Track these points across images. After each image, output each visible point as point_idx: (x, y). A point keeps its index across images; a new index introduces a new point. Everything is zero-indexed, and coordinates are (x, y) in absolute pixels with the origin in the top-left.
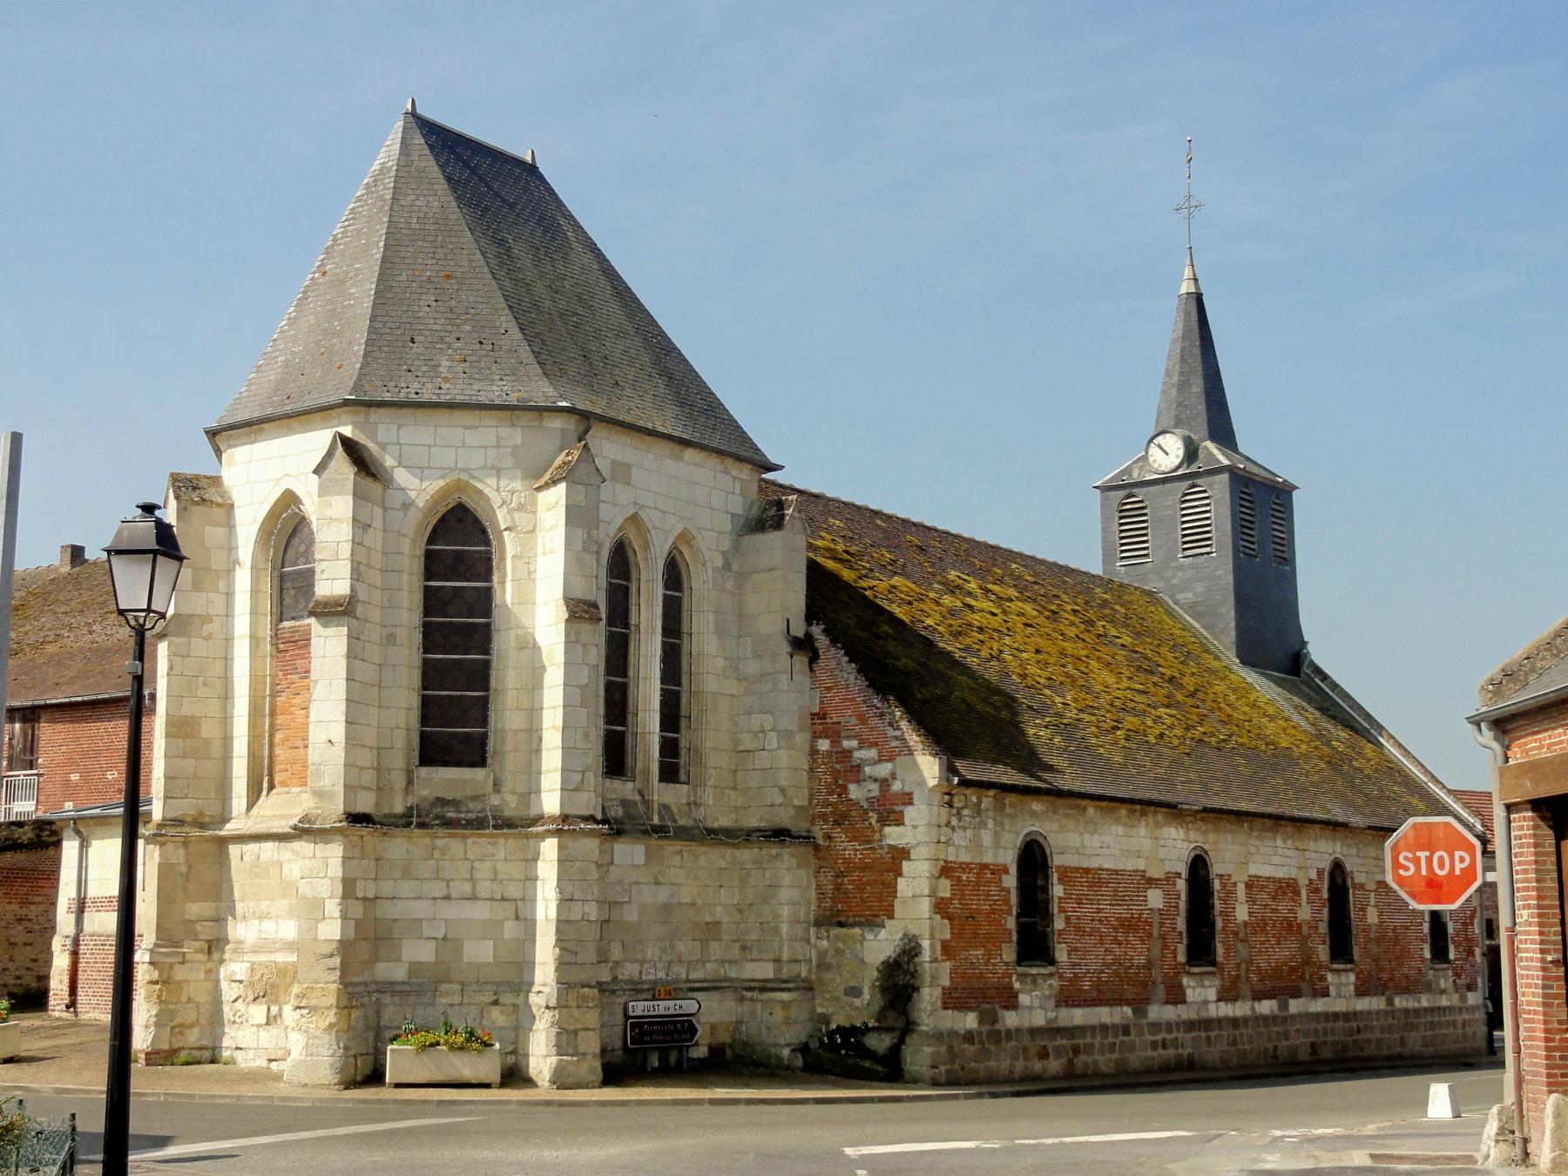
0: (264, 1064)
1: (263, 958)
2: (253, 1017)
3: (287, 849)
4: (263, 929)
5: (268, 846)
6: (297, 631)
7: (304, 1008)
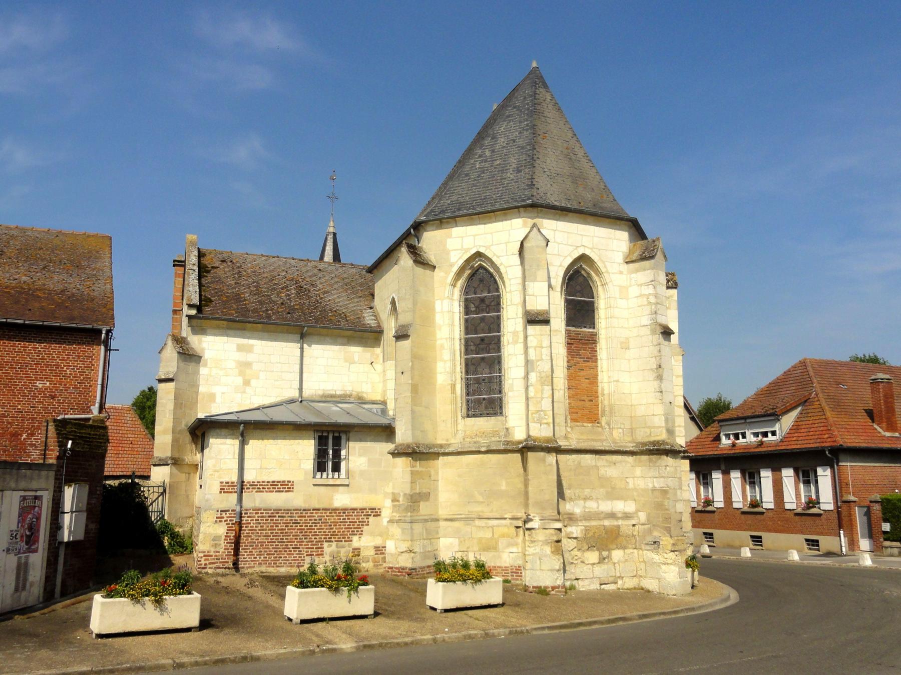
1: (594, 523)
3: (603, 460)
4: (587, 506)
5: (588, 457)
6: (580, 334)
7: (676, 551)
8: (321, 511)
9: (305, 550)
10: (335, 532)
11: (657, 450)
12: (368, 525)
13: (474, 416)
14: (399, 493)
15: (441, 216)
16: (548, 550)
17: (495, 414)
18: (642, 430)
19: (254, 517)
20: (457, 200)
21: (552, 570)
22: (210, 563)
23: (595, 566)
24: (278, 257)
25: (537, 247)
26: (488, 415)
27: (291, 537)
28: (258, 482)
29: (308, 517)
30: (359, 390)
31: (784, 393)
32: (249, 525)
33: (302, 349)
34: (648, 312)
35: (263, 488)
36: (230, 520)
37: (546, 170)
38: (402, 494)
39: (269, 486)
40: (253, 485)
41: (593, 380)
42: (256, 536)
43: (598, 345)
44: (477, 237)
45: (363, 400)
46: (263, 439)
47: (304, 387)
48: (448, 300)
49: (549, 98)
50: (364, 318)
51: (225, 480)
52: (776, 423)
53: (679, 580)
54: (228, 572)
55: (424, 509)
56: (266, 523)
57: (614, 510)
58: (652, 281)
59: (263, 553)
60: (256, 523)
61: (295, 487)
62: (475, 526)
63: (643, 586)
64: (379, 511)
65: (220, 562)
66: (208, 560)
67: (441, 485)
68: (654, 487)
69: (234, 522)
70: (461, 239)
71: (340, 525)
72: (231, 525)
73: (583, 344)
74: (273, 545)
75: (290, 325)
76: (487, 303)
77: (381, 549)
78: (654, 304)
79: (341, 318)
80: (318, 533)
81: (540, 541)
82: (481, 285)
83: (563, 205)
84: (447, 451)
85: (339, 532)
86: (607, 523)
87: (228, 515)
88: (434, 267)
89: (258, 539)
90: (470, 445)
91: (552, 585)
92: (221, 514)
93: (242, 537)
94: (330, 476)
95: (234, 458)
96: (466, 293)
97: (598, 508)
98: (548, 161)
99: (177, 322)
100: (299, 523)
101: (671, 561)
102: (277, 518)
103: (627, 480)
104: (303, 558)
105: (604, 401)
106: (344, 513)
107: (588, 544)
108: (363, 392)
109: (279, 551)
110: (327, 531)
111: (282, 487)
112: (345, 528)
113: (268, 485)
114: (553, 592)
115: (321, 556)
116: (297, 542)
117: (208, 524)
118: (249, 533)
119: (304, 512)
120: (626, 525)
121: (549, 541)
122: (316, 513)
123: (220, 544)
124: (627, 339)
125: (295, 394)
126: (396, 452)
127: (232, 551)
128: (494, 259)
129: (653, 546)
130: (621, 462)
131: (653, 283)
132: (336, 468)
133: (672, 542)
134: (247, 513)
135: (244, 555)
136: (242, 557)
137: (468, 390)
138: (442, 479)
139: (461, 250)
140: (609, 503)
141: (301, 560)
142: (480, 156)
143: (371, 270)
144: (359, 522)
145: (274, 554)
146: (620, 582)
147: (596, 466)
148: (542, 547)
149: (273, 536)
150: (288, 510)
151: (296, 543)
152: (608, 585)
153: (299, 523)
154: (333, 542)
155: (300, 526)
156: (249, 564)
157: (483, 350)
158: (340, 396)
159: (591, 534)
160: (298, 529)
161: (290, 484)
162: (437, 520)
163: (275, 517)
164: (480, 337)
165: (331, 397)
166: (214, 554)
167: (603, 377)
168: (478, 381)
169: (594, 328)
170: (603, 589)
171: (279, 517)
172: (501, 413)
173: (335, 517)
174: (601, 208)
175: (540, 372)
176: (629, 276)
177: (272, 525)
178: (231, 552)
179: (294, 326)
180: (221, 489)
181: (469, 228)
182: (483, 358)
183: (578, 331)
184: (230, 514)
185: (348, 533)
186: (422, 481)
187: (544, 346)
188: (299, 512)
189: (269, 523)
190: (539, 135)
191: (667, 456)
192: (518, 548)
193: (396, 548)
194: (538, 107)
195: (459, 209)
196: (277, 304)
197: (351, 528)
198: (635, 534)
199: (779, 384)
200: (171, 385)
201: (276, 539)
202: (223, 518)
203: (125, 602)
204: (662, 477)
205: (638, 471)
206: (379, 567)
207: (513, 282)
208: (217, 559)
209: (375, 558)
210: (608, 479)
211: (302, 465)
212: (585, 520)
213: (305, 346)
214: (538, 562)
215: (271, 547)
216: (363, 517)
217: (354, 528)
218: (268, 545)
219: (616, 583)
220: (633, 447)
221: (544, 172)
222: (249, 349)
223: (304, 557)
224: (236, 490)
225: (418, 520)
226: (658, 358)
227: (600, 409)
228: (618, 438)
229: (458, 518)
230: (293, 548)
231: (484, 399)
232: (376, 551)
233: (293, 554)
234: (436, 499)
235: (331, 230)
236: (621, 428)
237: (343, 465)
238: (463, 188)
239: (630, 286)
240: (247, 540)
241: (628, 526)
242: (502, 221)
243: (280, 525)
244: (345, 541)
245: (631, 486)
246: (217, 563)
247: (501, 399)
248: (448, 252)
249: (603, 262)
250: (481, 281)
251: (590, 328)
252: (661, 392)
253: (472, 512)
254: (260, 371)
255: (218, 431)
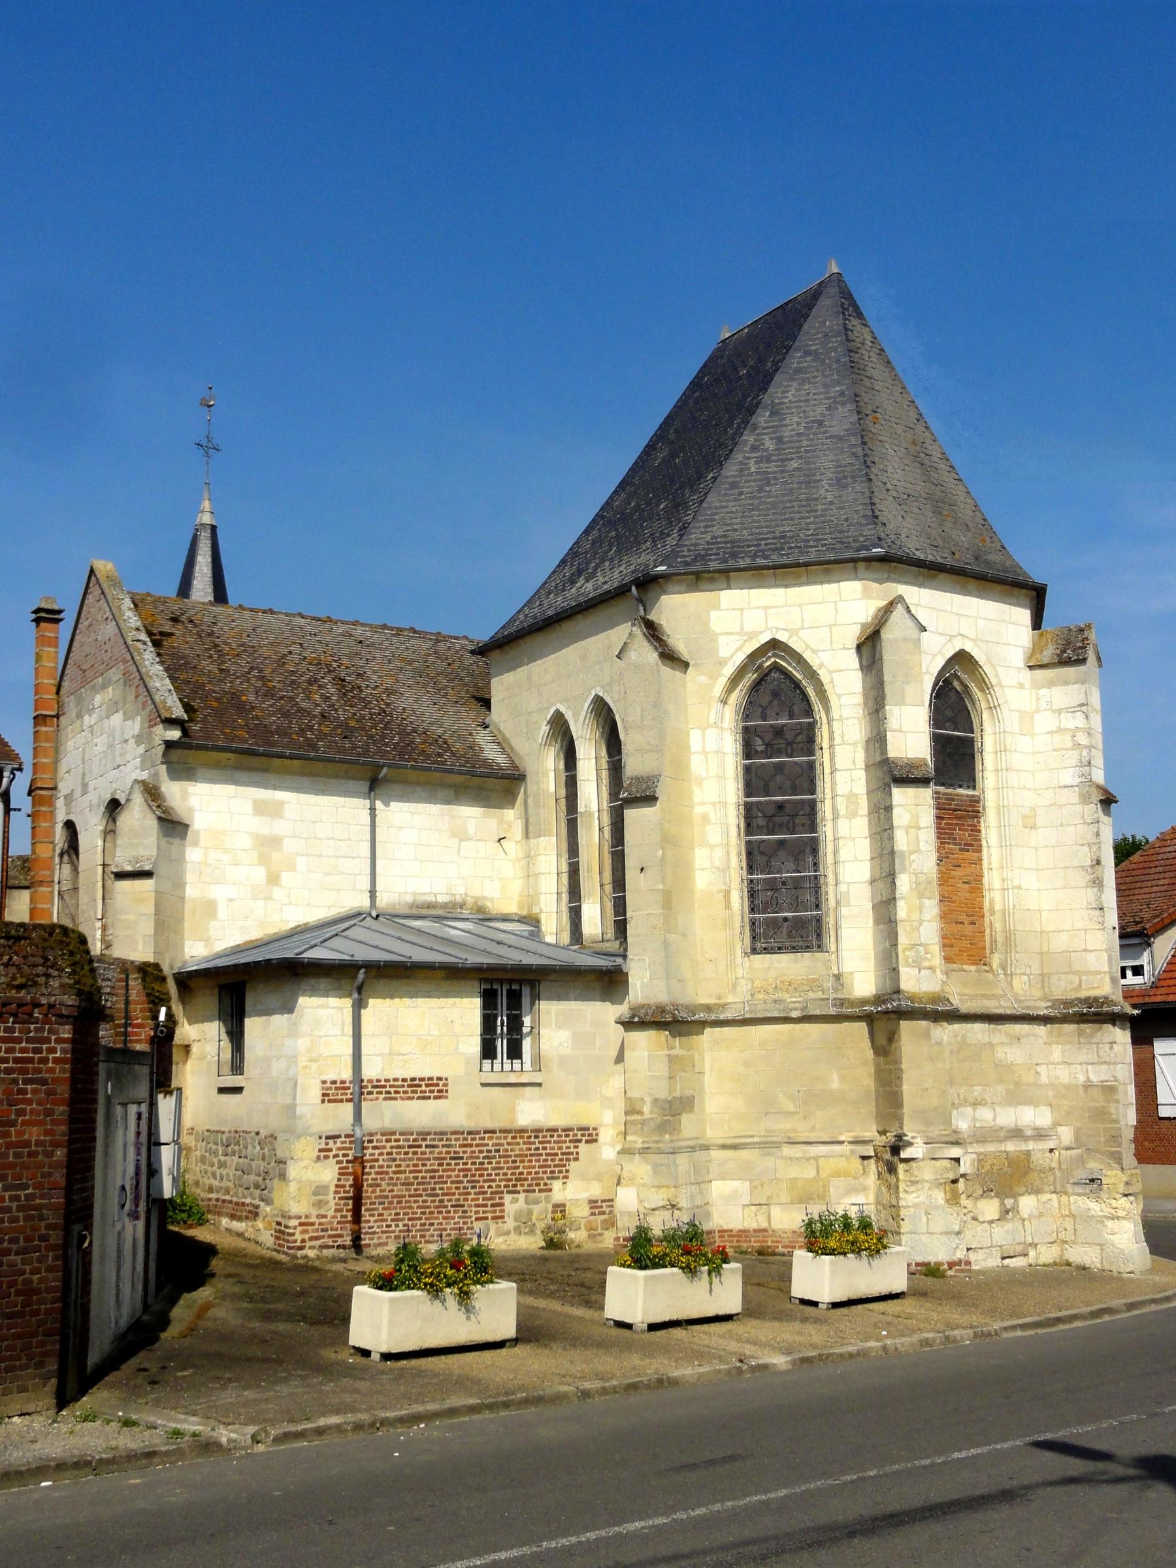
0: (998, 1262)
1: (991, 1148)
2: (983, 1214)
3: (1000, 1032)
4: (977, 1116)
5: (978, 1026)
6: (953, 800)
7: (1130, 1195)
8: (498, 1134)
9: (474, 1209)
10: (521, 1173)
11: (1096, 1014)
12: (576, 1159)
13: (766, 951)
14: (643, 1099)
15: (698, 567)
16: (940, 1197)
17: (808, 948)
18: (1063, 977)
19: (384, 1147)
20: (724, 536)
21: (947, 1233)
22: (311, 1239)
23: (993, 1225)
24: (272, 612)
25: (905, 639)
26: (794, 949)
27: (449, 1185)
28: (387, 1081)
29: (477, 1145)
30: (477, 893)
31: (1147, 890)
32: (377, 1164)
33: (373, 810)
34: (1074, 761)
35: (396, 1092)
36: (344, 1155)
37: (889, 486)
38: (648, 1100)
39: (406, 1089)
40: (378, 1085)
41: (975, 884)
42: (388, 1185)
43: (982, 820)
44: (770, 611)
45: (484, 913)
46: (392, 997)
47: (379, 887)
48: (715, 730)
49: (869, 338)
50: (482, 751)
51: (330, 1077)
52: (1144, 950)
53: (1137, 1246)
54: (342, 1255)
55: (688, 1125)
56: (404, 1160)
57: (1019, 1123)
58: (1083, 705)
59: (401, 1216)
60: (388, 1160)
61: (449, 1088)
62: (782, 1157)
63: (1071, 1260)
64: (594, 1133)
65: (329, 1236)
66: (306, 1232)
67: (709, 1081)
68: (1088, 1080)
69: (350, 1158)
70: (739, 612)
71: (531, 1161)
72: (345, 1165)
73: (958, 818)
74: (418, 1201)
75: (356, 763)
76: (787, 737)
77: (599, 1204)
78: (1086, 747)
79: (440, 747)
80: (493, 1177)
81: (927, 1181)
82: (776, 702)
83: (930, 558)
84: (722, 1017)
85: (529, 1173)
86: (1011, 1147)
87: (339, 1145)
88: (686, 665)
89: (392, 1191)
90: (768, 1006)
91: (948, 1259)
92: (327, 1144)
93: (365, 1188)
94: (497, 1067)
95: (343, 1035)
96: (746, 717)
97: (994, 1120)
98: (890, 469)
99: (46, 742)
100: (462, 1158)
101: (1124, 1213)
102: (423, 1149)
103: (1039, 1069)
104: (469, 1225)
105: (994, 923)
106: (537, 1137)
107: (982, 1186)
108: (485, 898)
109: (430, 1213)
110: (509, 1172)
111: (428, 1089)
112: (540, 1167)
113: (403, 1086)
114: (950, 1273)
115: (500, 1221)
116: (459, 1194)
117: (305, 1163)
118: (376, 1179)
119: (469, 1137)
120: (1040, 1150)
121: (942, 1181)
122: (490, 1138)
123: (327, 1202)
124: (1033, 809)
125: (364, 902)
126: (636, 1019)
127: (349, 1214)
128: (807, 656)
129: (1089, 1188)
130: (1028, 1035)
131: (1084, 708)
132: (515, 1052)
133: (1125, 1179)
134: (370, 1141)
135: (369, 1221)
136: (367, 1225)
137: (752, 902)
138: (711, 1071)
139: (741, 633)
140: (1012, 1110)
141: (468, 1229)
142: (754, 448)
143: (482, 651)
144: (563, 1154)
145: (420, 1219)
146: (1032, 1253)
147: (990, 1043)
148: (930, 1192)
149: (418, 1184)
150: (442, 1133)
151: (457, 1196)
152: (1014, 1260)
153: (462, 1158)
154: (519, 1192)
155: (463, 1164)
156: (378, 1238)
157: (781, 826)
158: (444, 906)
159: (987, 1168)
160: (460, 1170)
161: (441, 1083)
162: (706, 1148)
163: (420, 1146)
164: (776, 802)
165: (428, 907)
166: (317, 1221)
167: (992, 879)
168: (772, 885)
169: (974, 788)
170: (1008, 1266)
171: (427, 1146)
172: (819, 946)
173: (522, 1146)
174: (987, 563)
175: (916, 874)
176: (1033, 691)
177: (415, 1162)
178: (346, 1217)
179: (341, 761)
180: (324, 1095)
181: (755, 592)
182: (782, 843)
183: (951, 794)
184: (343, 1142)
185: (545, 1176)
186: (683, 1074)
187: (922, 826)
188: (461, 1137)
189: (410, 1159)
190: (867, 415)
191: (1114, 1025)
192: (867, 1196)
193: (641, 1201)
194: (856, 357)
195: (734, 555)
196: (315, 716)
197: (549, 1166)
198: (1053, 1165)
199: (1134, 873)
200: (146, 885)
201: (424, 1190)
202: (331, 1150)
203: (419, 1296)
204: (1105, 1062)
205: (1057, 1052)
206: (598, 1238)
207: (845, 700)
208: (323, 1230)
209: (589, 1222)
210: (1009, 1067)
211: (460, 1046)
212: (978, 1142)
213: (378, 804)
214: (924, 1220)
215: (415, 1205)
216: (568, 1144)
217: (555, 1166)
218: (410, 1202)
219: (1026, 1255)
220: (1047, 1008)
221: (888, 490)
222: (275, 811)
223: (472, 1222)
224: (349, 1096)
225: (682, 1148)
226: (1094, 848)
227: (987, 938)
228: (1021, 992)
229: (746, 1144)
230: (452, 1206)
231: (785, 919)
232: (591, 1208)
233: (453, 1218)
234: (702, 1109)
235: (207, 519)
236: (1025, 974)
237: (527, 1045)
238: (732, 512)
239: (1038, 711)
240: (373, 1192)
241: (1043, 1151)
242: (822, 583)
243: (428, 1163)
244: (540, 1191)
245: (1044, 1079)
246: (323, 1237)
247: (818, 920)
248: (713, 638)
249: (993, 666)
250: (776, 694)
251: (968, 787)
252: (1101, 909)
253: (774, 1131)
254: (298, 854)
255: (312, 981)
